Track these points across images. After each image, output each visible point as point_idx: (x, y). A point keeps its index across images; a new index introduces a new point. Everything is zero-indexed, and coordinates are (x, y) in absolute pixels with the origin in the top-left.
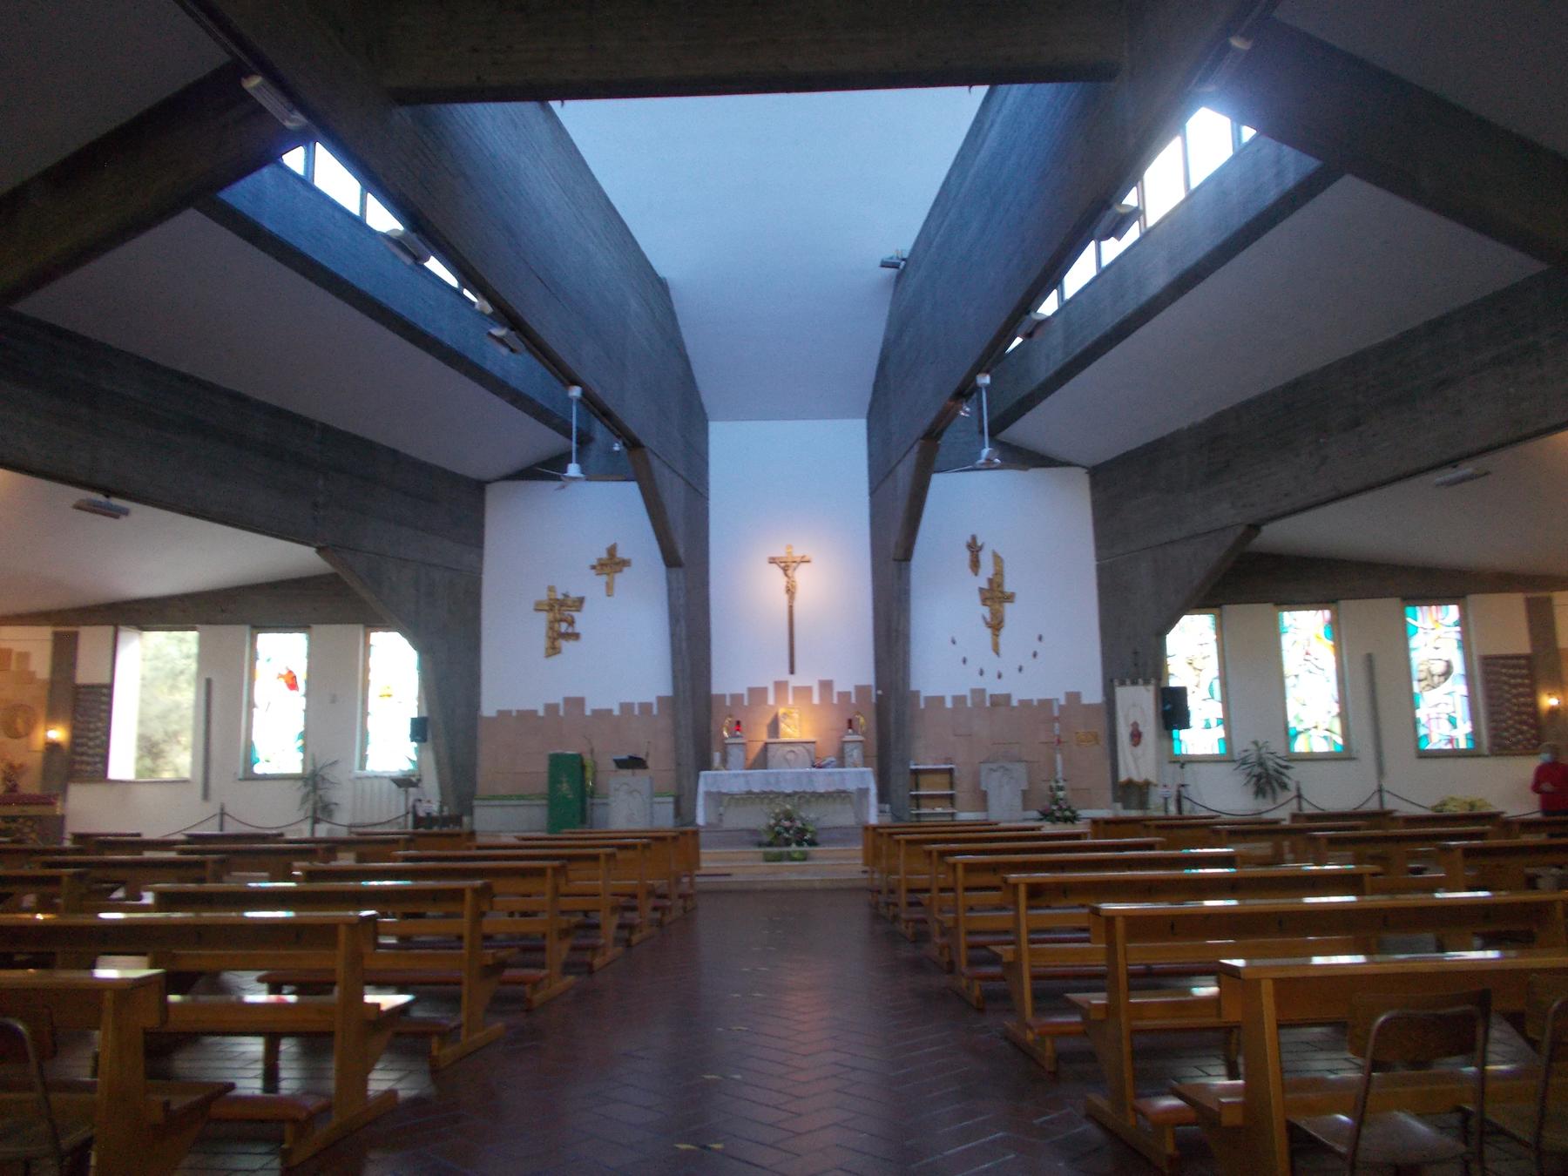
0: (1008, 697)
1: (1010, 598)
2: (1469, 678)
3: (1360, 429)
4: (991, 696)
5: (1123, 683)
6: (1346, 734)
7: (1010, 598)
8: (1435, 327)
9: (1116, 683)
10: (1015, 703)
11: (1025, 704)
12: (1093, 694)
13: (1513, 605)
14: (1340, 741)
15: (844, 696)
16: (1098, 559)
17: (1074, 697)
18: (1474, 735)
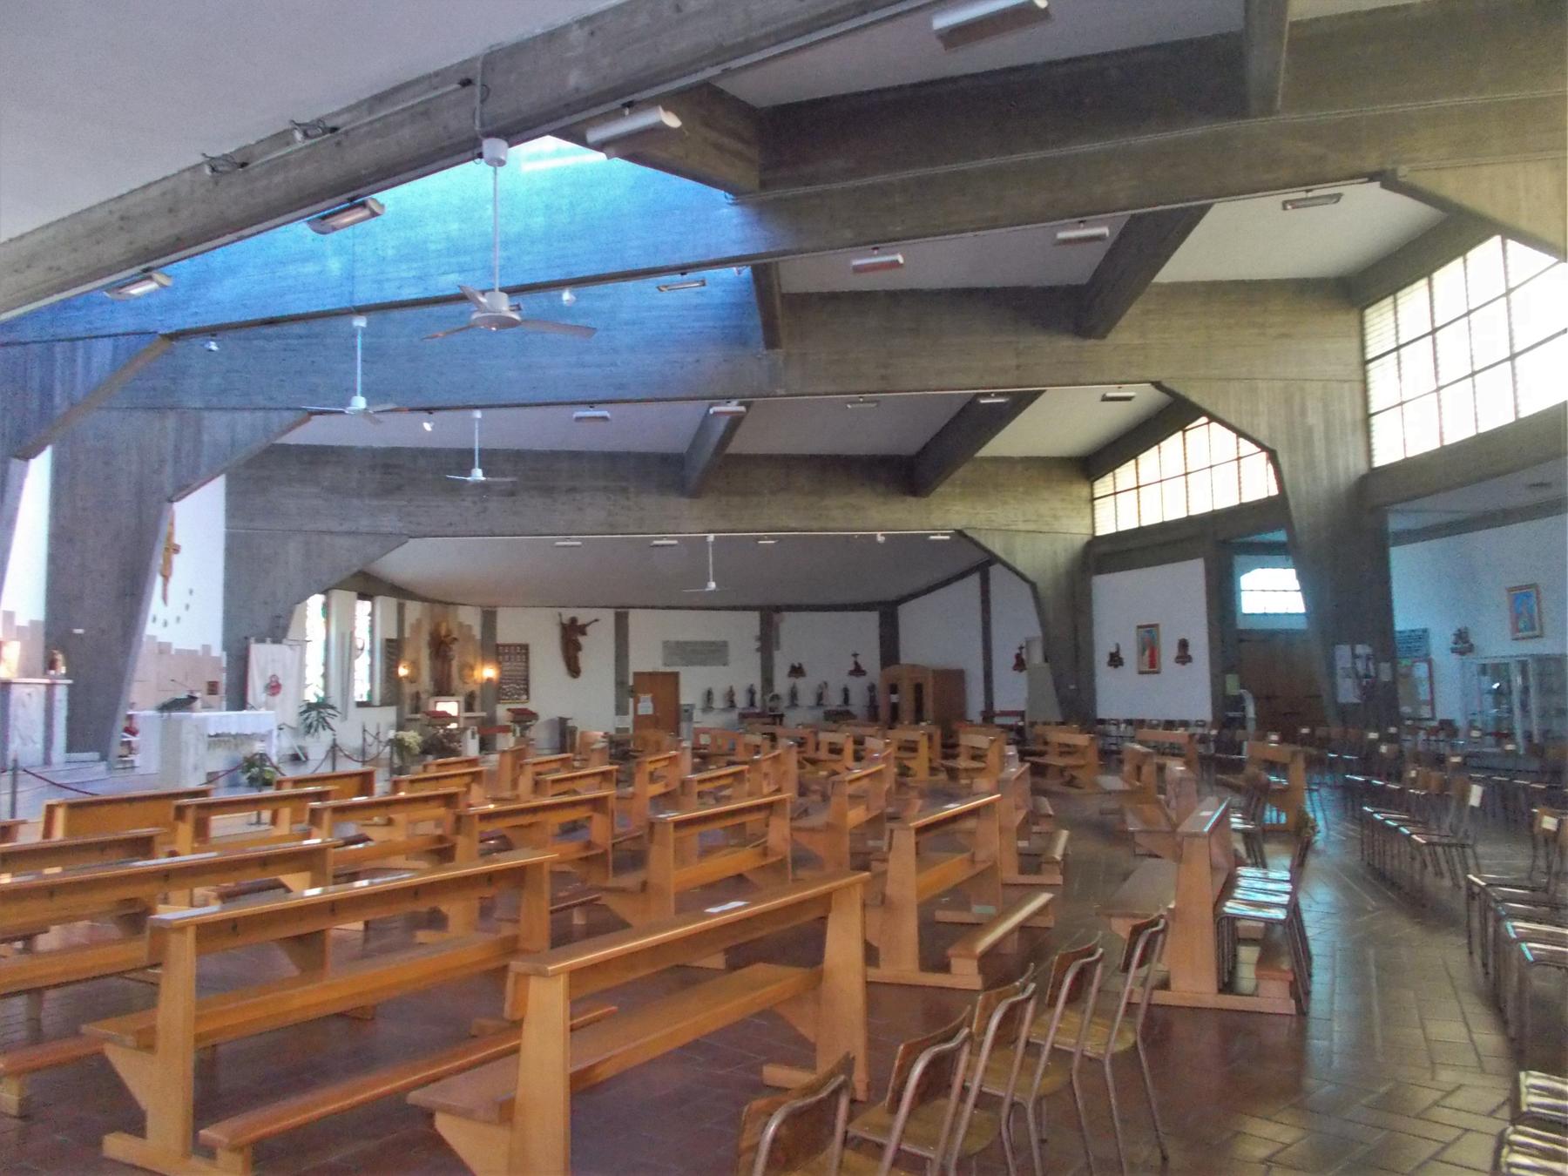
0: (169, 645)
1: (176, 550)
2: (372, 652)
3: (514, 498)
4: (160, 643)
5: (261, 640)
6: (326, 688)
7: (176, 550)
8: (575, 456)
9: (252, 640)
10: (173, 652)
11: (179, 651)
12: (217, 651)
13: (392, 602)
14: (321, 694)
15: (20, 629)
16: (227, 527)
17: (206, 648)
18: (371, 694)
